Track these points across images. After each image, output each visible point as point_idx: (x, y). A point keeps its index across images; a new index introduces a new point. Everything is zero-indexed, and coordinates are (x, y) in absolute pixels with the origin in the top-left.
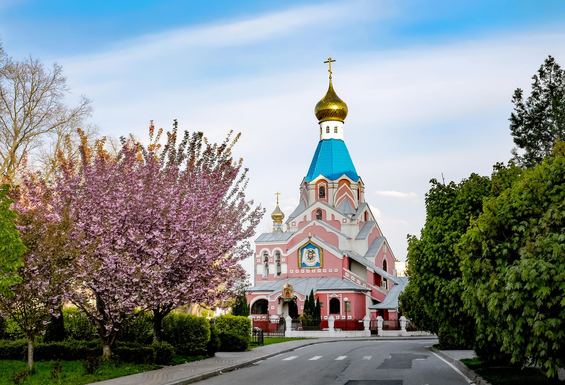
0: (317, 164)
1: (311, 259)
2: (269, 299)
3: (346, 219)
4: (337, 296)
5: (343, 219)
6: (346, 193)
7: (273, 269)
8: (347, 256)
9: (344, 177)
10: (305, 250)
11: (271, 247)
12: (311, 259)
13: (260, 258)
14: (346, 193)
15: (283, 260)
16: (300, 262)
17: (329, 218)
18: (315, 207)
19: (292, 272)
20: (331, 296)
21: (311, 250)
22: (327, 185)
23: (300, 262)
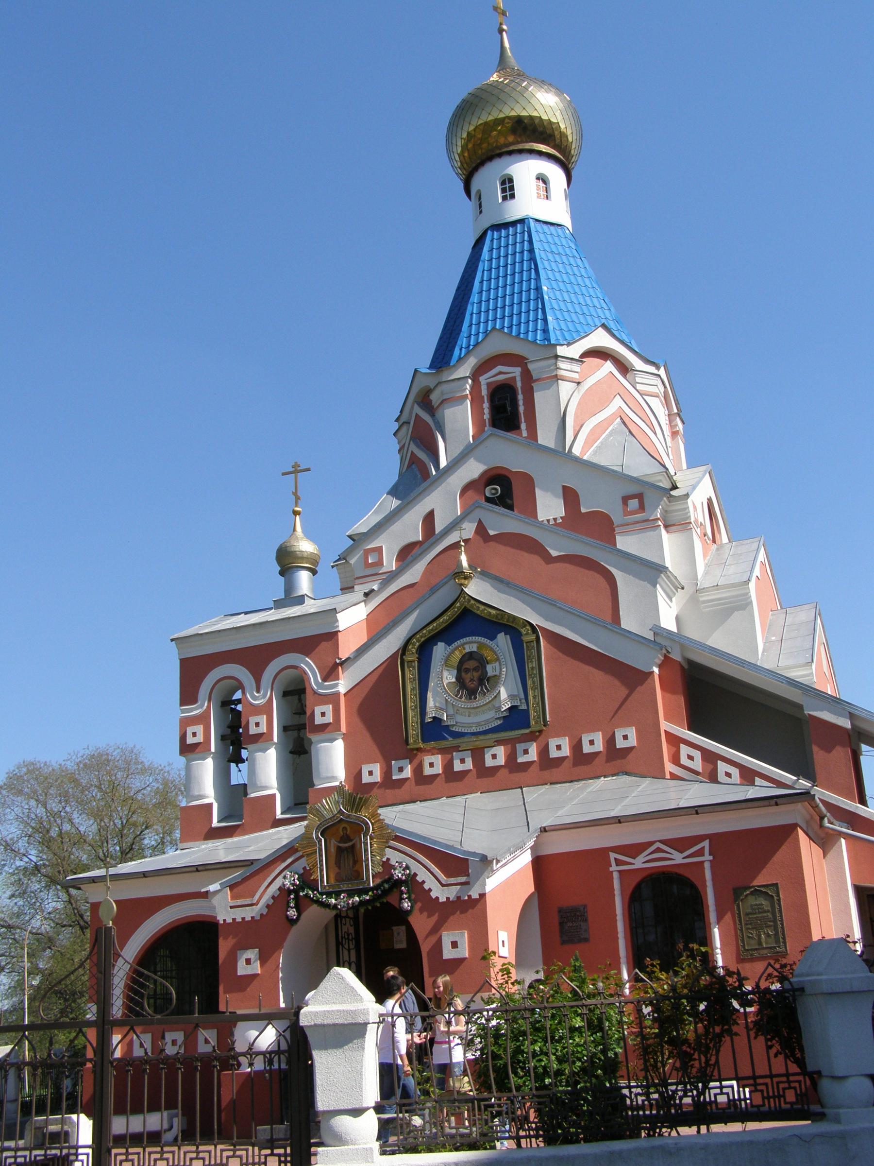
0: (472, 308)
1: (472, 694)
2: (224, 909)
3: (640, 497)
4: (678, 858)
5: (625, 500)
6: (618, 402)
7: (267, 769)
8: (676, 656)
9: (600, 339)
10: (440, 650)
11: (255, 658)
12: (472, 694)
13: (203, 719)
14: (618, 402)
15: (322, 714)
16: (412, 716)
17: (549, 507)
18: (473, 469)
19: (372, 772)
20: (639, 862)
21: (470, 644)
22: (527, 376)
23: (412, 716)
